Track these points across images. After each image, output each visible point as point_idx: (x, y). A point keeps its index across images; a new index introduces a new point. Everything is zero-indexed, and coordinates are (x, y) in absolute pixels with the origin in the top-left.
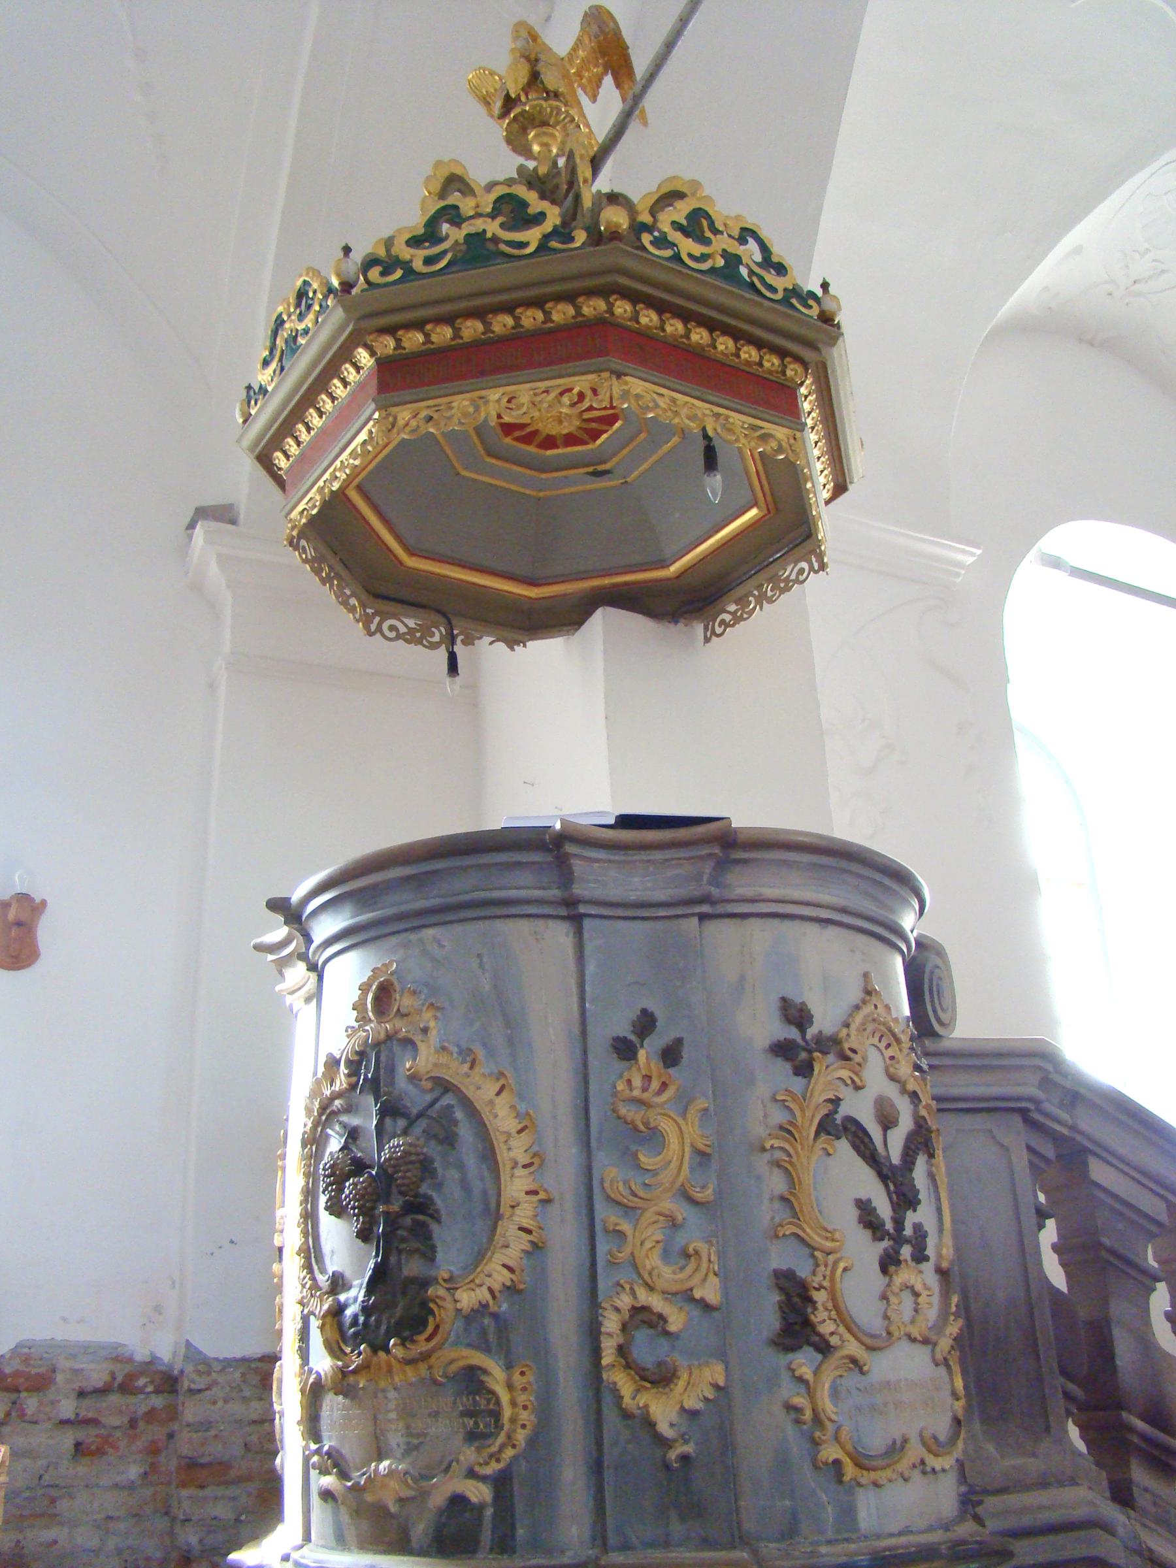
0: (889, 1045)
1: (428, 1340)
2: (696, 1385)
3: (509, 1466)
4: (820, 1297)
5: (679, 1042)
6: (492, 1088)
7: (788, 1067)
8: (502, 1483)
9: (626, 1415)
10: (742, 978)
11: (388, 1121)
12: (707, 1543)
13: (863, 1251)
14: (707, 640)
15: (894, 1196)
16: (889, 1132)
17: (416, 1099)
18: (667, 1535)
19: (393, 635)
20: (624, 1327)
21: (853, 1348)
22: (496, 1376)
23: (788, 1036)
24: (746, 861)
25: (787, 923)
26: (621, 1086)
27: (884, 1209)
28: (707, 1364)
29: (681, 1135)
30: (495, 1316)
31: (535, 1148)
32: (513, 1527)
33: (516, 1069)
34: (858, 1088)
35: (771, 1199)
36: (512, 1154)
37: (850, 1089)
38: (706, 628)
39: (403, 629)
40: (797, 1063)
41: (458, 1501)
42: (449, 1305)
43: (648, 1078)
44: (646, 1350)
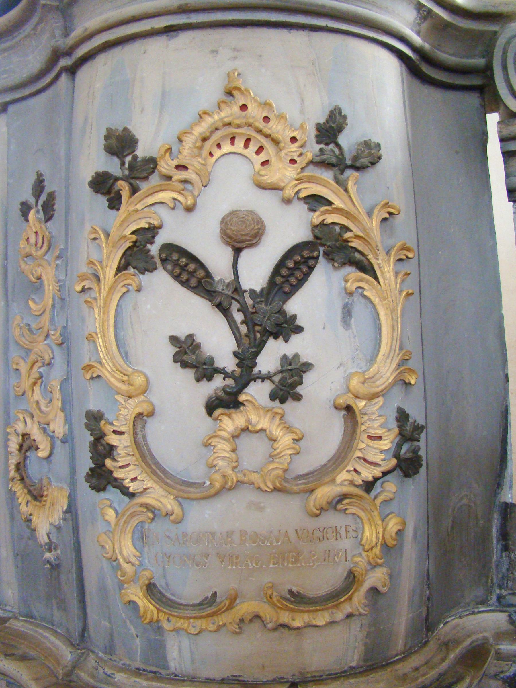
0: (260, 149)
13: (182, 395)
15: (244, 329)
16: (245, 255)
27: (219, 342)
34: (189, 209)
37: (180, 212)
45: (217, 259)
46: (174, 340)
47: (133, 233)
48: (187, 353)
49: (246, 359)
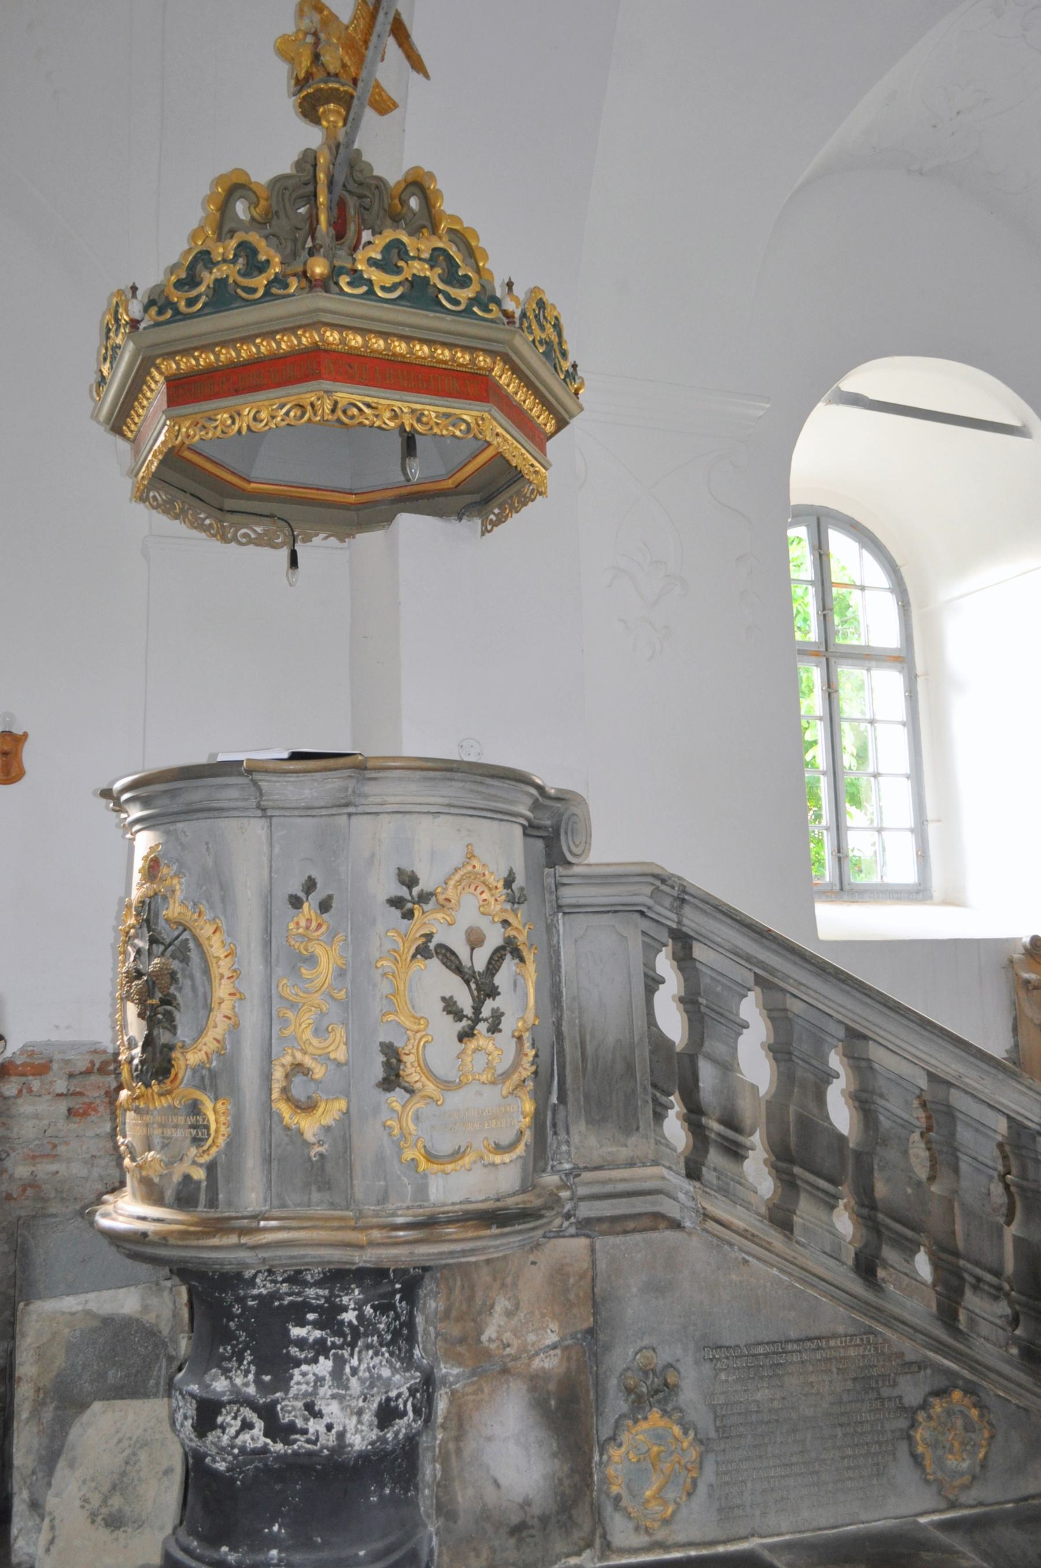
1: (172, 1082)
2: (330, 1112)
3: (215, 1158)
4: (410, 1059)
5: (330, 897)
6: (209, 930)
7: (398, 913)
8: (211, 1168)
9: (287, 1128)
10: (373, 855)
11: (154, 946)
12: (333, 1205)
14: (483, 534)
15: (475, 993)
16: (475, 951)
17: (167, 933)
18: (309, 1199)
19: (244, 540)
20: (287, 1076)
22: (208, 1105)
23: (400, 894)
24: (375, 779)
25: (408, 816)
26: (292, 926)
27: (465, 1002)
28: (337, 1098)
29: (327, 959)
30: (210, 1070)
31: (236, 966)
32: (217, 1194)
33: (225, 917)
35: (381, 999)
36: (221, 971)
38: (482, 524)
40: (405, 910)
41: (187, 1178)
42: (182, 1063)
43: (309, 921)
44: (299, 1089)
45: (462, 951)
46: (443, 999)
47: (422, 936)
48: (450, 1007)
49: (477, 1010)
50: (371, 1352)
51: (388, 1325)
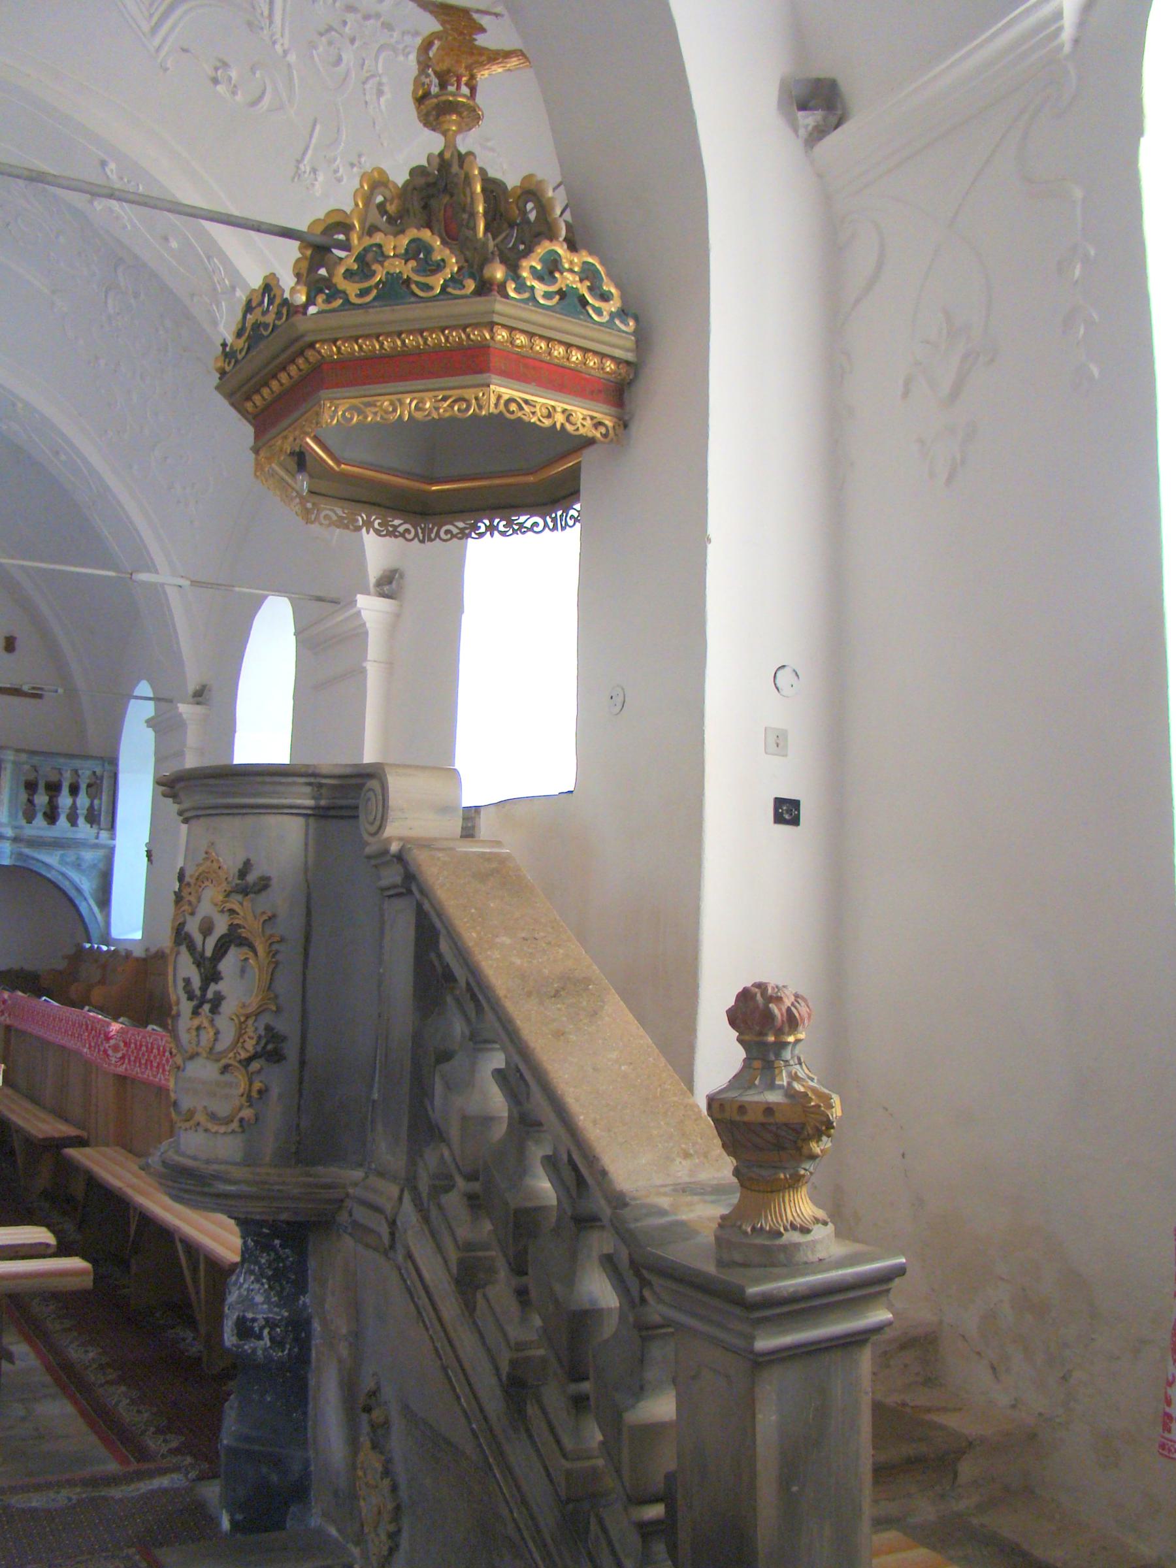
21: (179, 1060)
27: (196, 983)
39: (455, 531)
50: (252, 1278)
51: (270, 1263)
